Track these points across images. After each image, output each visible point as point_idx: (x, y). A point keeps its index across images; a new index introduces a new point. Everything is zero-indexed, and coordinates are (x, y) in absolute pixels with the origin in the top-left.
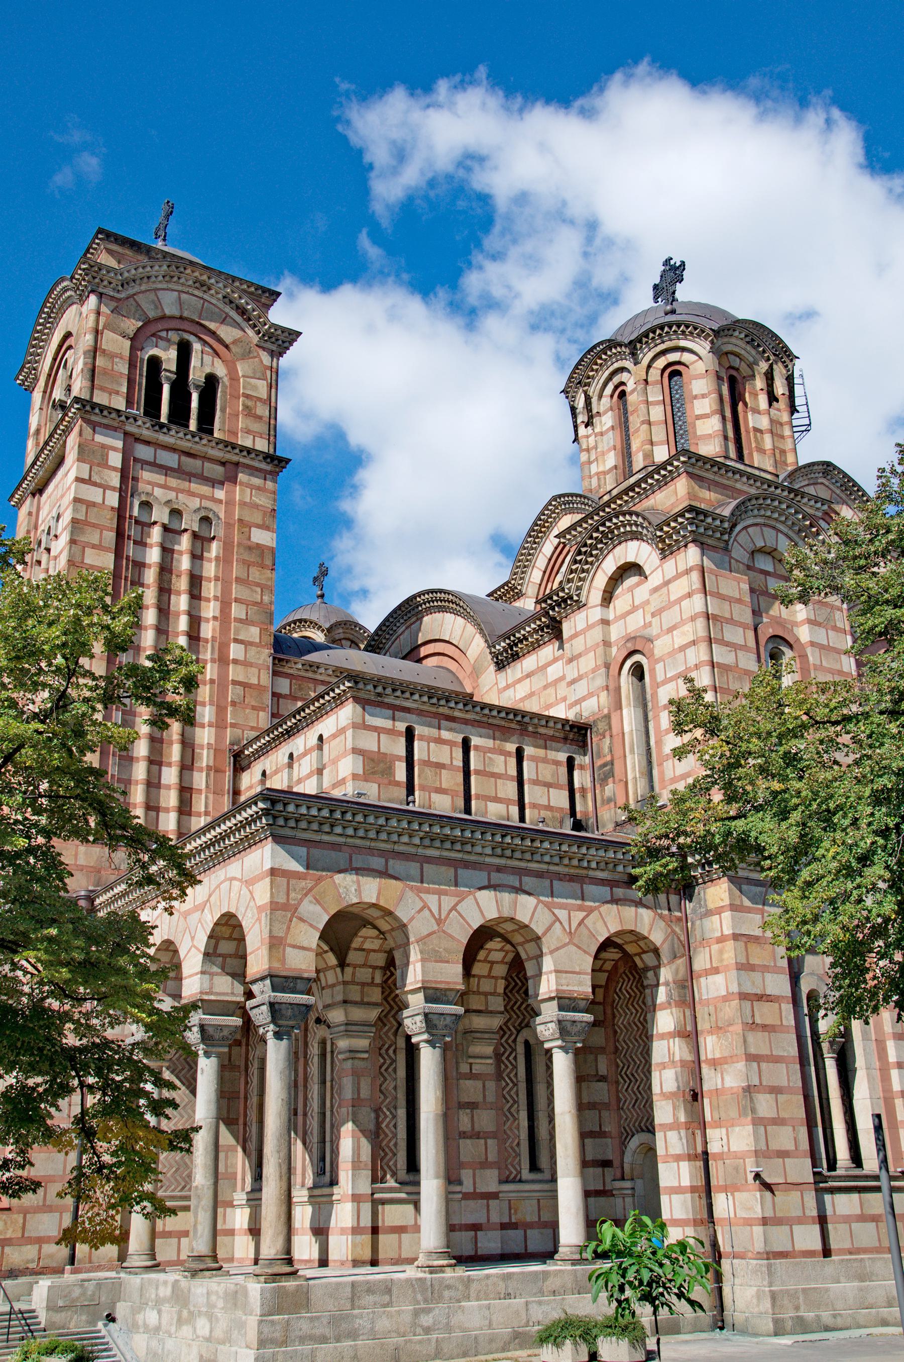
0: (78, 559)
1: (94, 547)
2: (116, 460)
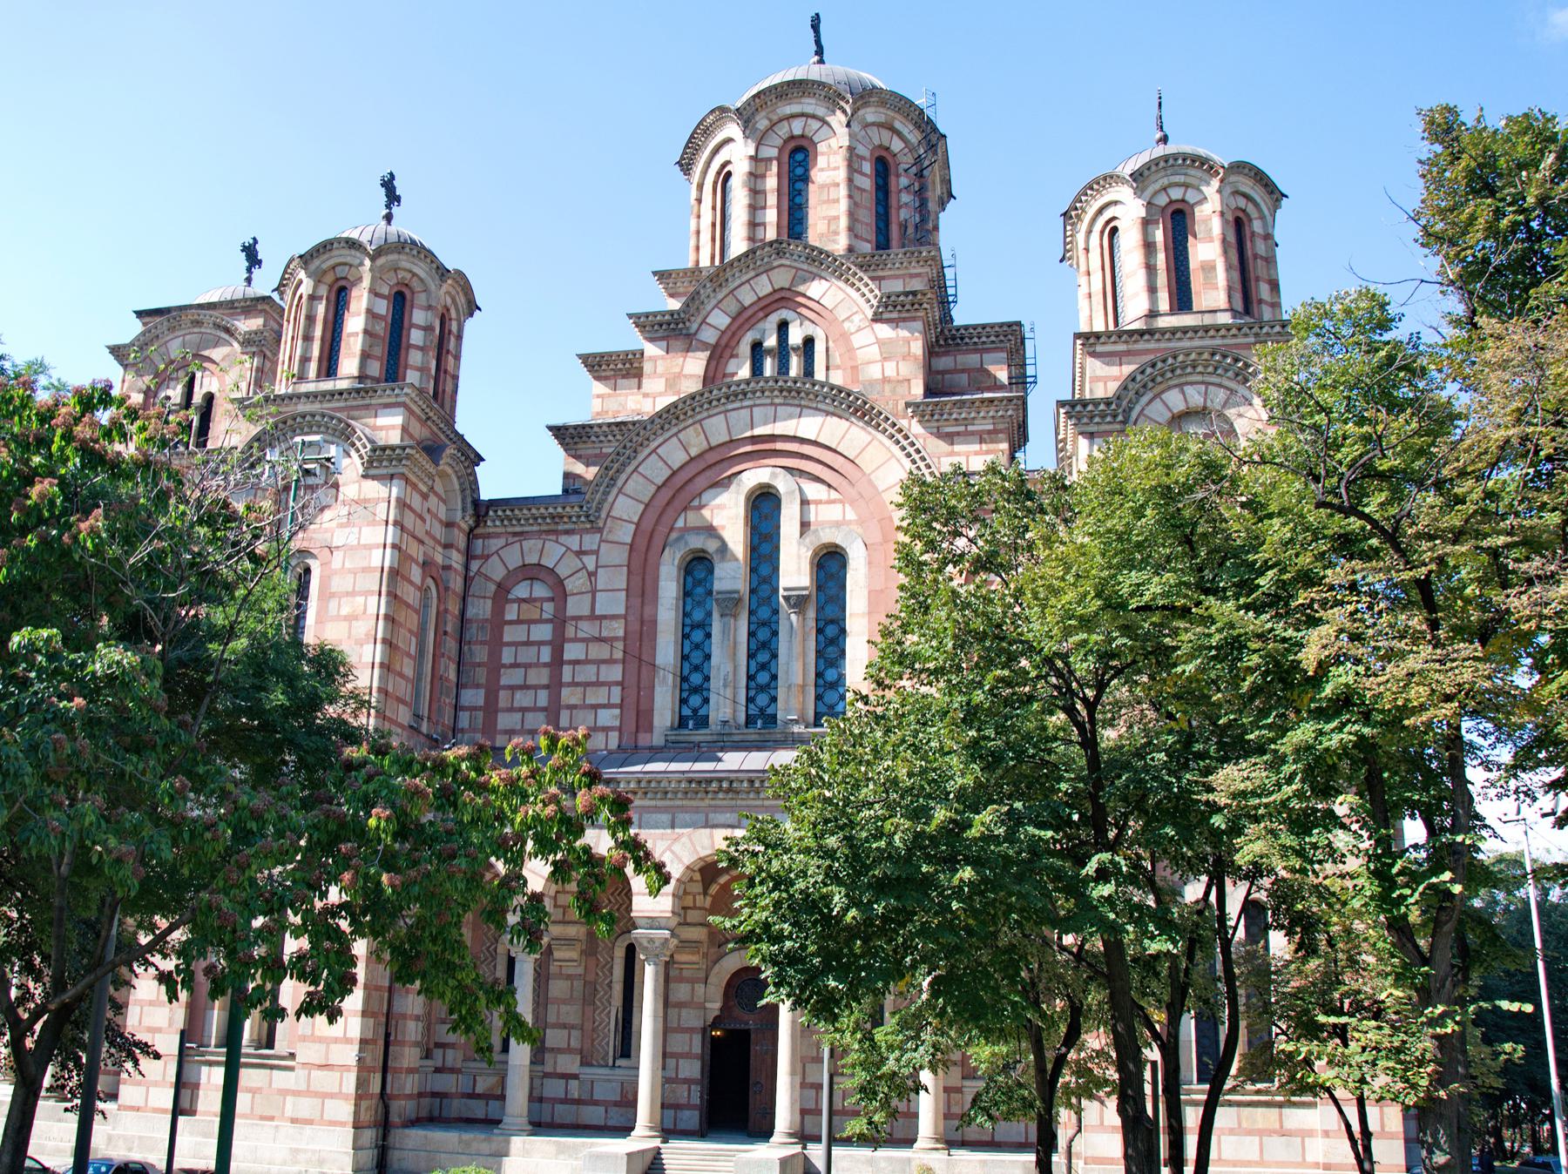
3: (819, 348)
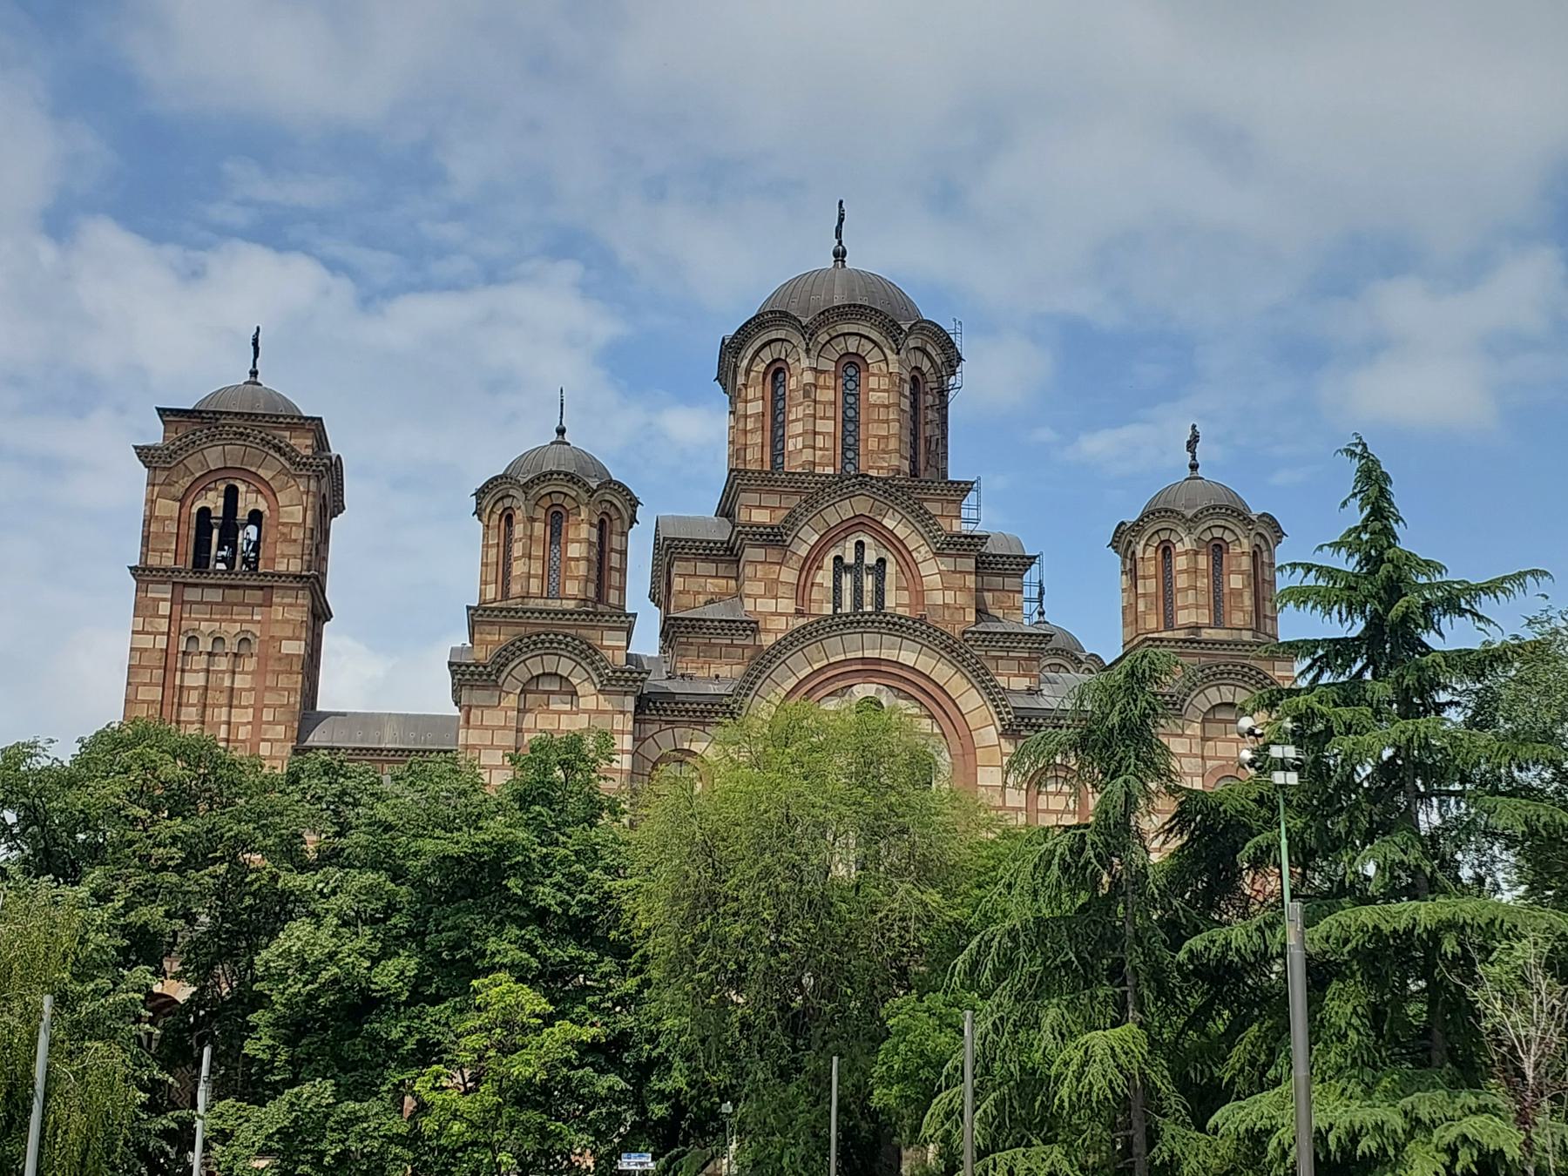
0: (132, 697)
1: (145, 684)
2: (164, 608)
3: (891, 568)
